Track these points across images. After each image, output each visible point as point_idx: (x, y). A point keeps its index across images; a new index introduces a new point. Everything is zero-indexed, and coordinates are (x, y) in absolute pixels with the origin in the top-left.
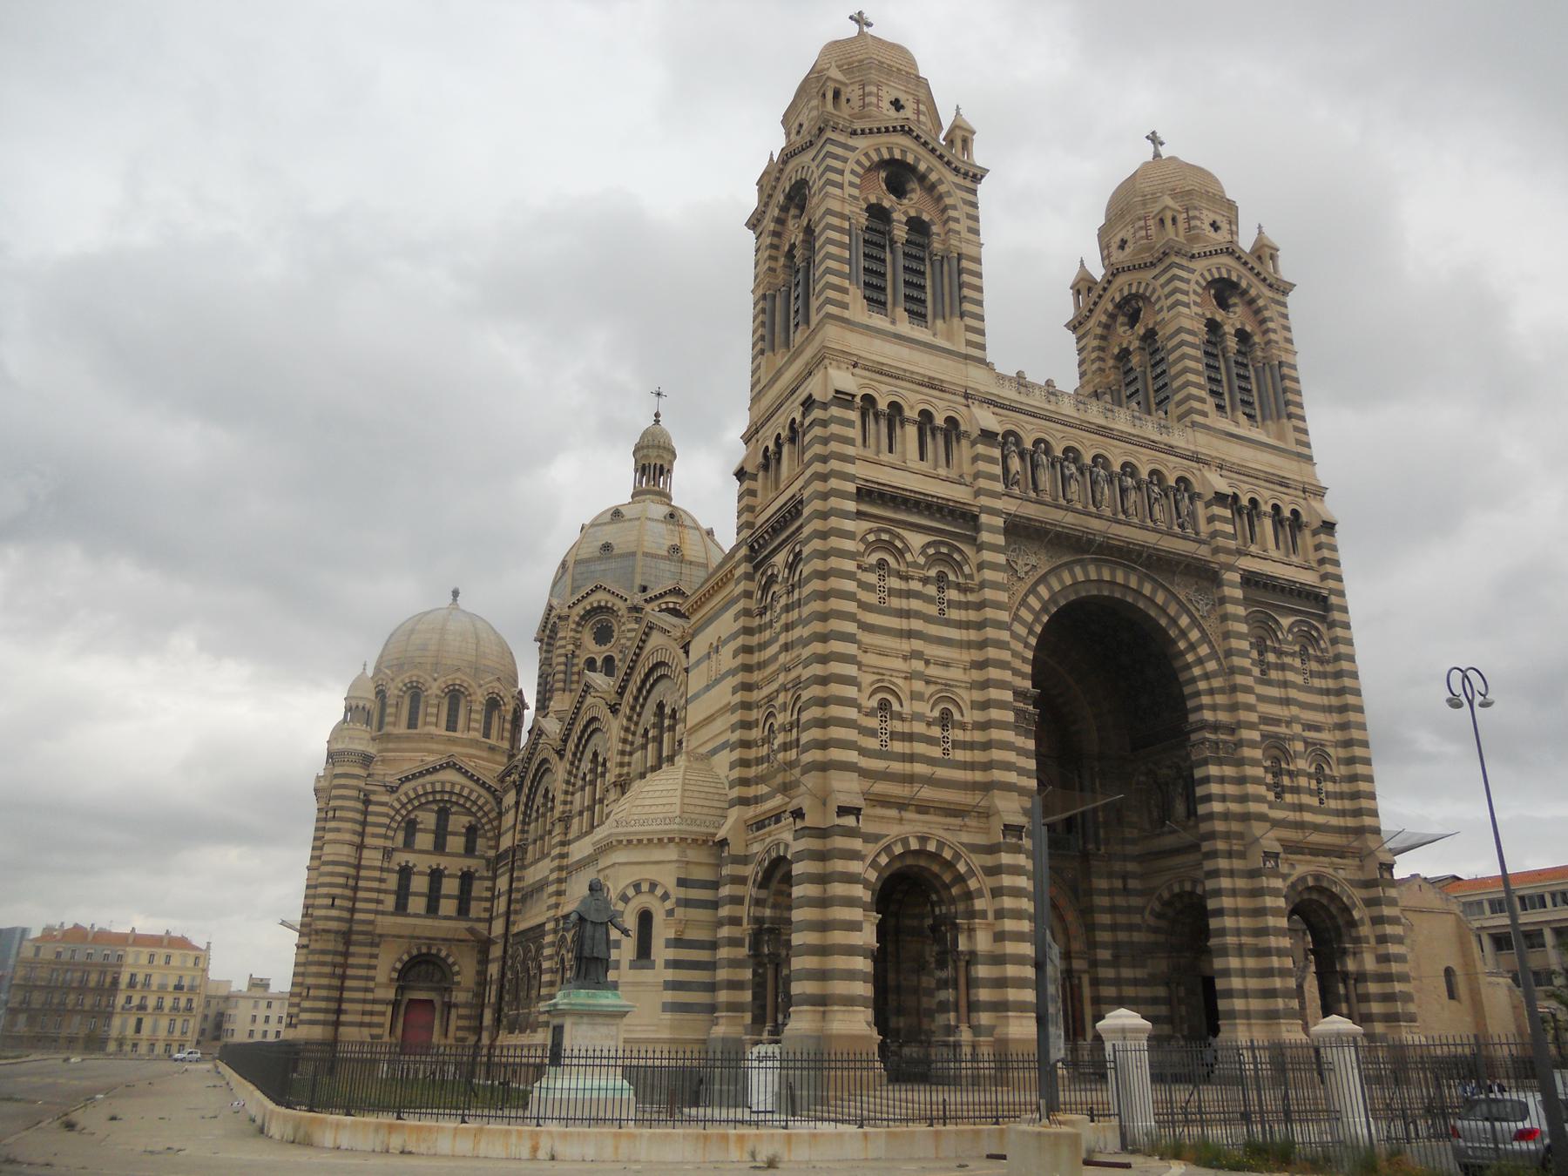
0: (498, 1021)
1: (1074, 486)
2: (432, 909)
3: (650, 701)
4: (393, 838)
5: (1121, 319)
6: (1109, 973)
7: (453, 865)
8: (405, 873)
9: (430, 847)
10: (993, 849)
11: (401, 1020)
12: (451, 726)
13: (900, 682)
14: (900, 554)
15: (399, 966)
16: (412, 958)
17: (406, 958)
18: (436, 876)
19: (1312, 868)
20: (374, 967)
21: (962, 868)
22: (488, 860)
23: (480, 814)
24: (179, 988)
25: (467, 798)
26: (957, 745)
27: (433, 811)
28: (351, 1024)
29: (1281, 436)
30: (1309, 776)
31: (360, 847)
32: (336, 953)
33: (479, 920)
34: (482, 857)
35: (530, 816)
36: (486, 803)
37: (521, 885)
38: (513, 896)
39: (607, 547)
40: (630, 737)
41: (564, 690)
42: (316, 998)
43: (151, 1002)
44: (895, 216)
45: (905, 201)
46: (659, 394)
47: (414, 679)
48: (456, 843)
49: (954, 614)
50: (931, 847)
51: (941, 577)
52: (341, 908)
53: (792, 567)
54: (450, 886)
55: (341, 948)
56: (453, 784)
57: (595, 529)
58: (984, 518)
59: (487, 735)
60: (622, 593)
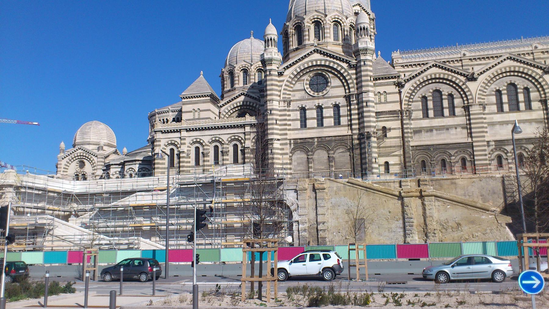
37: (412, 126)
38: (405, 131)
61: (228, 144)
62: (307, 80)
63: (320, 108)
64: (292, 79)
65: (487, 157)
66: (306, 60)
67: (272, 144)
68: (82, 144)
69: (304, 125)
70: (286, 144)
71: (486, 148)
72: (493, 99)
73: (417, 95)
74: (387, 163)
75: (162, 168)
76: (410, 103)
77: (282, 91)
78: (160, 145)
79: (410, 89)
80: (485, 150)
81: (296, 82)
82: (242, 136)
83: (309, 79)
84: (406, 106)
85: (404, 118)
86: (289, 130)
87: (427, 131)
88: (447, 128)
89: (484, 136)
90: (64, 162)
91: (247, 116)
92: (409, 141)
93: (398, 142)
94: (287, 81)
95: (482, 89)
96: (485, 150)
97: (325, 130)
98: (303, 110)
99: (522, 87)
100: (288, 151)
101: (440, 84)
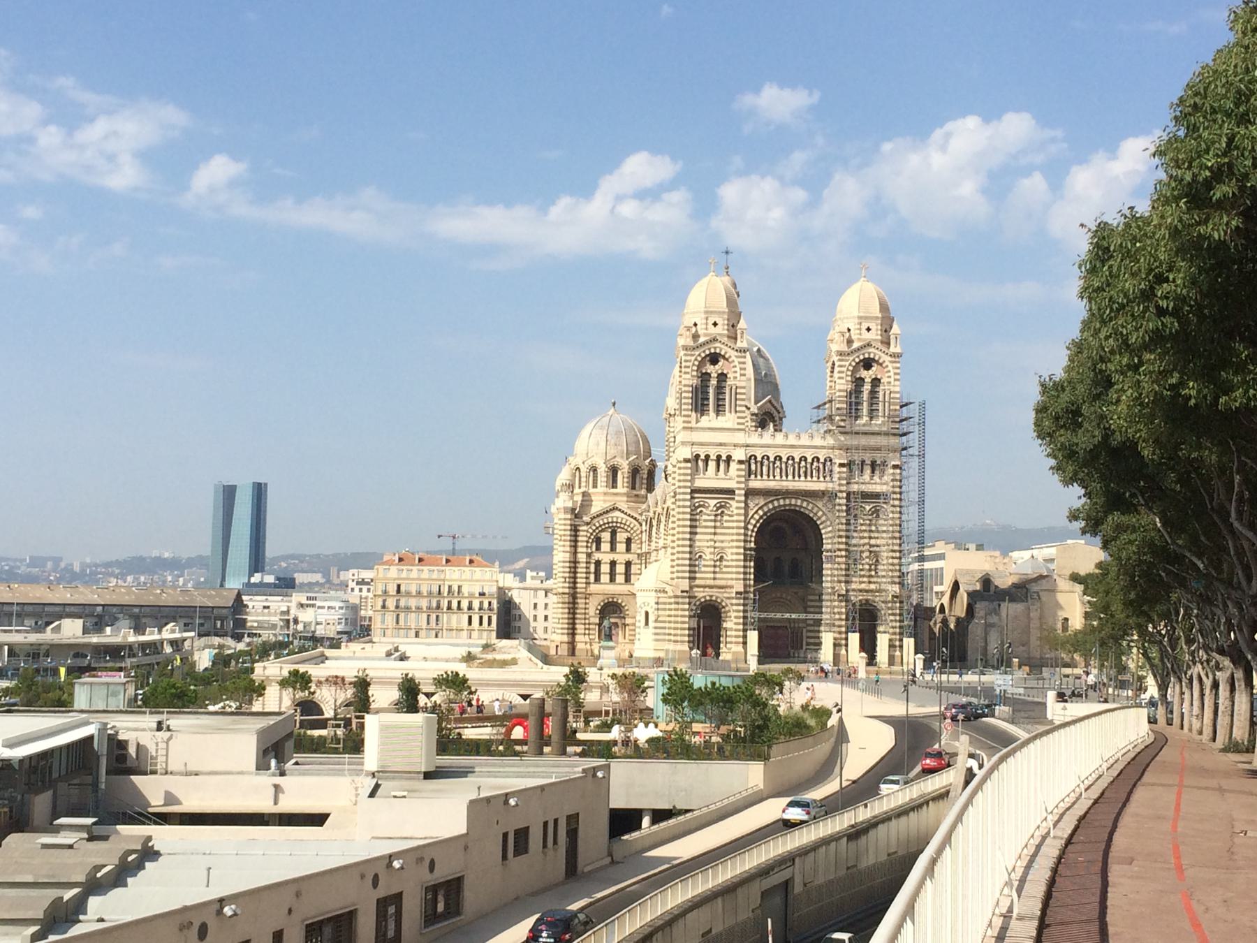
2: (612, 579)
4: (591, 547)
6: (812, 628)
7: (621, 558)
9: (609, 550)
10: (733, 598)
12: (614, 485)
13: (706, 549)
14: (707, 507)
15: (599, 607)
16: (605, 604)
17: (602, 604)
18: (613, 564)
19: (865, 597)
21: (724, 604)
22: (638, 554)
23: (632, 532)
24: (482, 594)
25: (625, 524)
26: (726, 566)
28: (581, 634)
30: (870, 565)
31: (575, 553)
32: (569, 603)
34: (635, 553)
36: (635, 526)
42: (562, 623)
43: (465, 605)
44: (712, 375)
45: (717, 366)
46: (727, 253)
48: (621, 547)
49: (725, 524)
50: (714, 598)
51: (723, 512)
52: (569, 583)
54: (620, 569)
55: (571, 601)
56: (617, 518)
58: (737, 492)
59: (633, 488)
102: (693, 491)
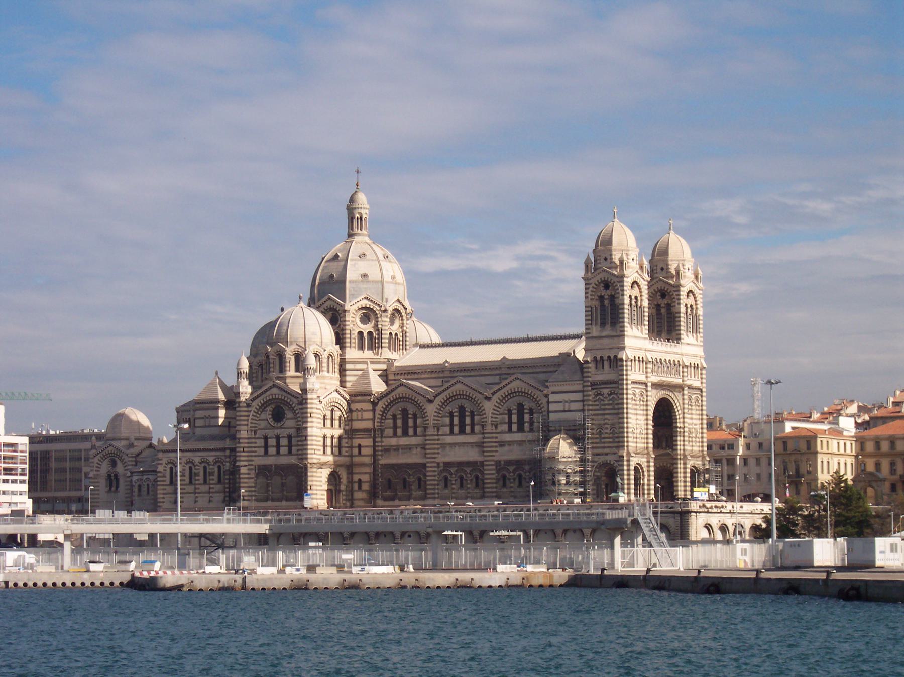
0: (373, 495)
1: (660, 369)
3: (510, 400)
5: (659, 294)
8: (325, 437)
11: (334, 497)
20: (321, 477)
27: (329, 410)
29: (697, 339)
33: (345, 456)
35: (385, 417)
37: (383, 444)
38: (377, 449)
39: (365, 276)
40: (499, 410)
41: (350, 347)
46: (358, 172)
47: (316, 350)
53: (609, 395)
57: (354, 262)
60: (379, 302)
61: (213, 465)
62: (270, 411)
63: (278, 438)
64: (258, 410)
65: (436, 478)
66: (268, 393)
67: (239, 470)
68: (113, 440)
69: (266, 452)
70: (252, 469)
71: (436, 469)
72: (447, 420)
73: (389, 413)
74: (360, 481)
75: (163, 485)
76: (383, 421)
77: (250, 421)
78: (161, 464)
79: (382, 407)
80: (434, 471)
81: (262, 411)
82: (223, 458)
83: (272, 409)
84: (379, 424)
85: (377, 436)
86: (255, 456)
87: (395, 450)
88: (409, 448)
89: (435, 458)
90: (96, 460)
91: (228, 440)
92: (379, 460)
93: (368, 460)
94: (254, 412)
95: (438, 411)
96: (434, 471)
97: (282, 457)
98: (266, 438)
99: (469, 411)
100: (253, 476)
101: (408, 403)
102: (633, 382)
